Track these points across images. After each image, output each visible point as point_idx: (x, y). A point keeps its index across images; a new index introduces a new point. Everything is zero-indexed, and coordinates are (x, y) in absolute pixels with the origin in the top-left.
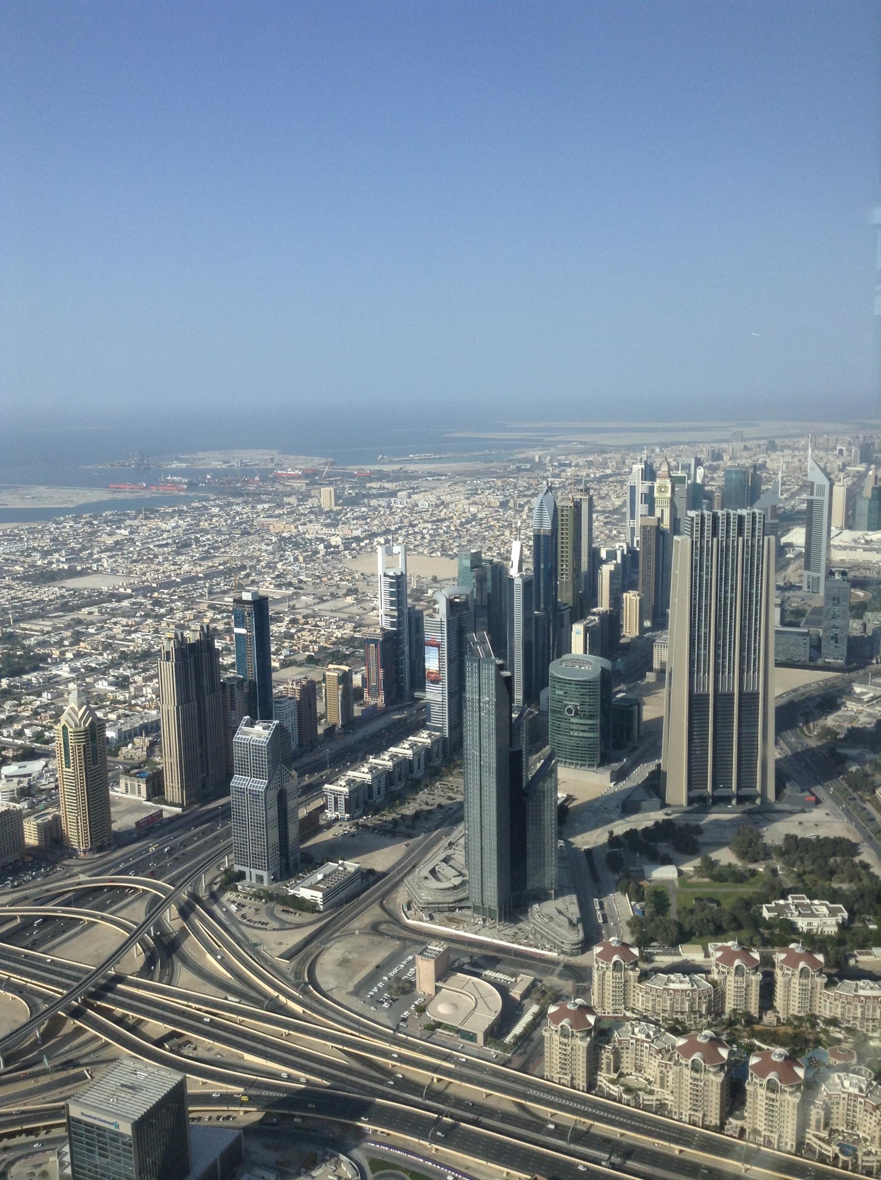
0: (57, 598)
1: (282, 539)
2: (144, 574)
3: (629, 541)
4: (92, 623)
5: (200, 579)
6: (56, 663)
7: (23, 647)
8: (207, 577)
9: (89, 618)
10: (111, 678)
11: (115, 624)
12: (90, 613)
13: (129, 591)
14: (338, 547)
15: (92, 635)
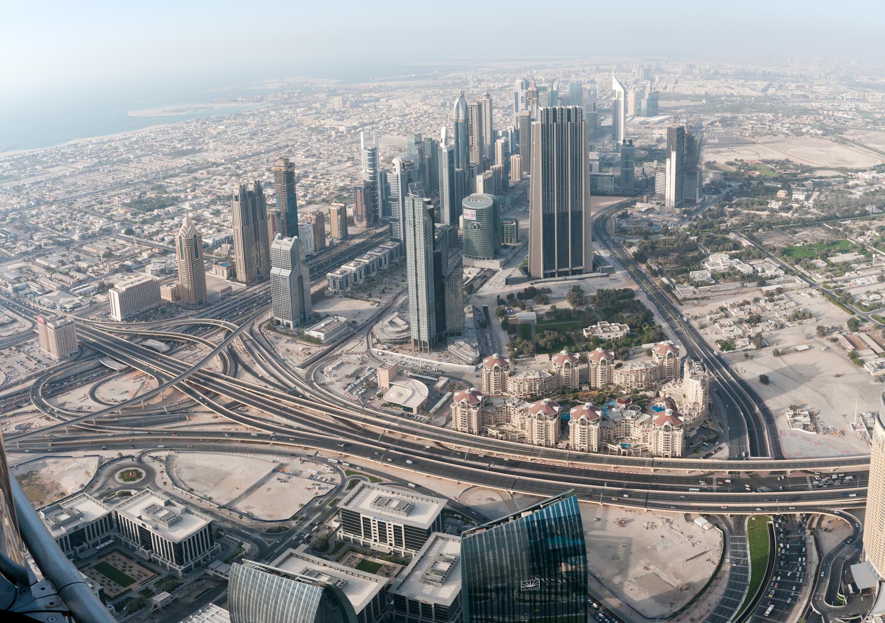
0: (185, 165)
1: (311, 129)
2: (232, 151)
3: (515, 125)
4: (203, 179)
5: (262, 153)
6: (183, 201)
7: (166, 192)
8: (267, 152)
9: (201, 176)
10: (211, 210)
11: (215, 180)
12: (202, 174)
13: (223, 161)
14: (343, 132)
15: (202, 186)
